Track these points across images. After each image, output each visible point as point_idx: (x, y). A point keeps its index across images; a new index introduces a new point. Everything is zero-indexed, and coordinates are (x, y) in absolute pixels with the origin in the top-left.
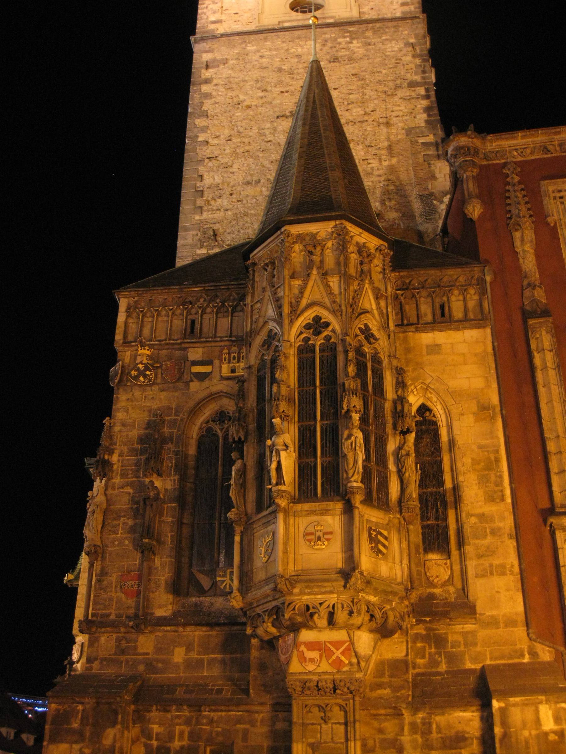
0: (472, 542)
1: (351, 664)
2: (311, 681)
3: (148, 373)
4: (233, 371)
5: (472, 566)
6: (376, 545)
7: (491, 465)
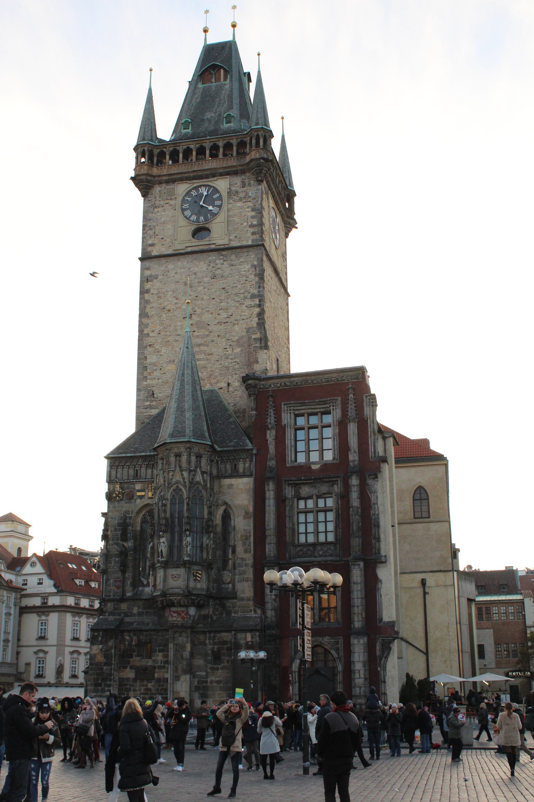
5: (237, 577)
7: (247, 538)
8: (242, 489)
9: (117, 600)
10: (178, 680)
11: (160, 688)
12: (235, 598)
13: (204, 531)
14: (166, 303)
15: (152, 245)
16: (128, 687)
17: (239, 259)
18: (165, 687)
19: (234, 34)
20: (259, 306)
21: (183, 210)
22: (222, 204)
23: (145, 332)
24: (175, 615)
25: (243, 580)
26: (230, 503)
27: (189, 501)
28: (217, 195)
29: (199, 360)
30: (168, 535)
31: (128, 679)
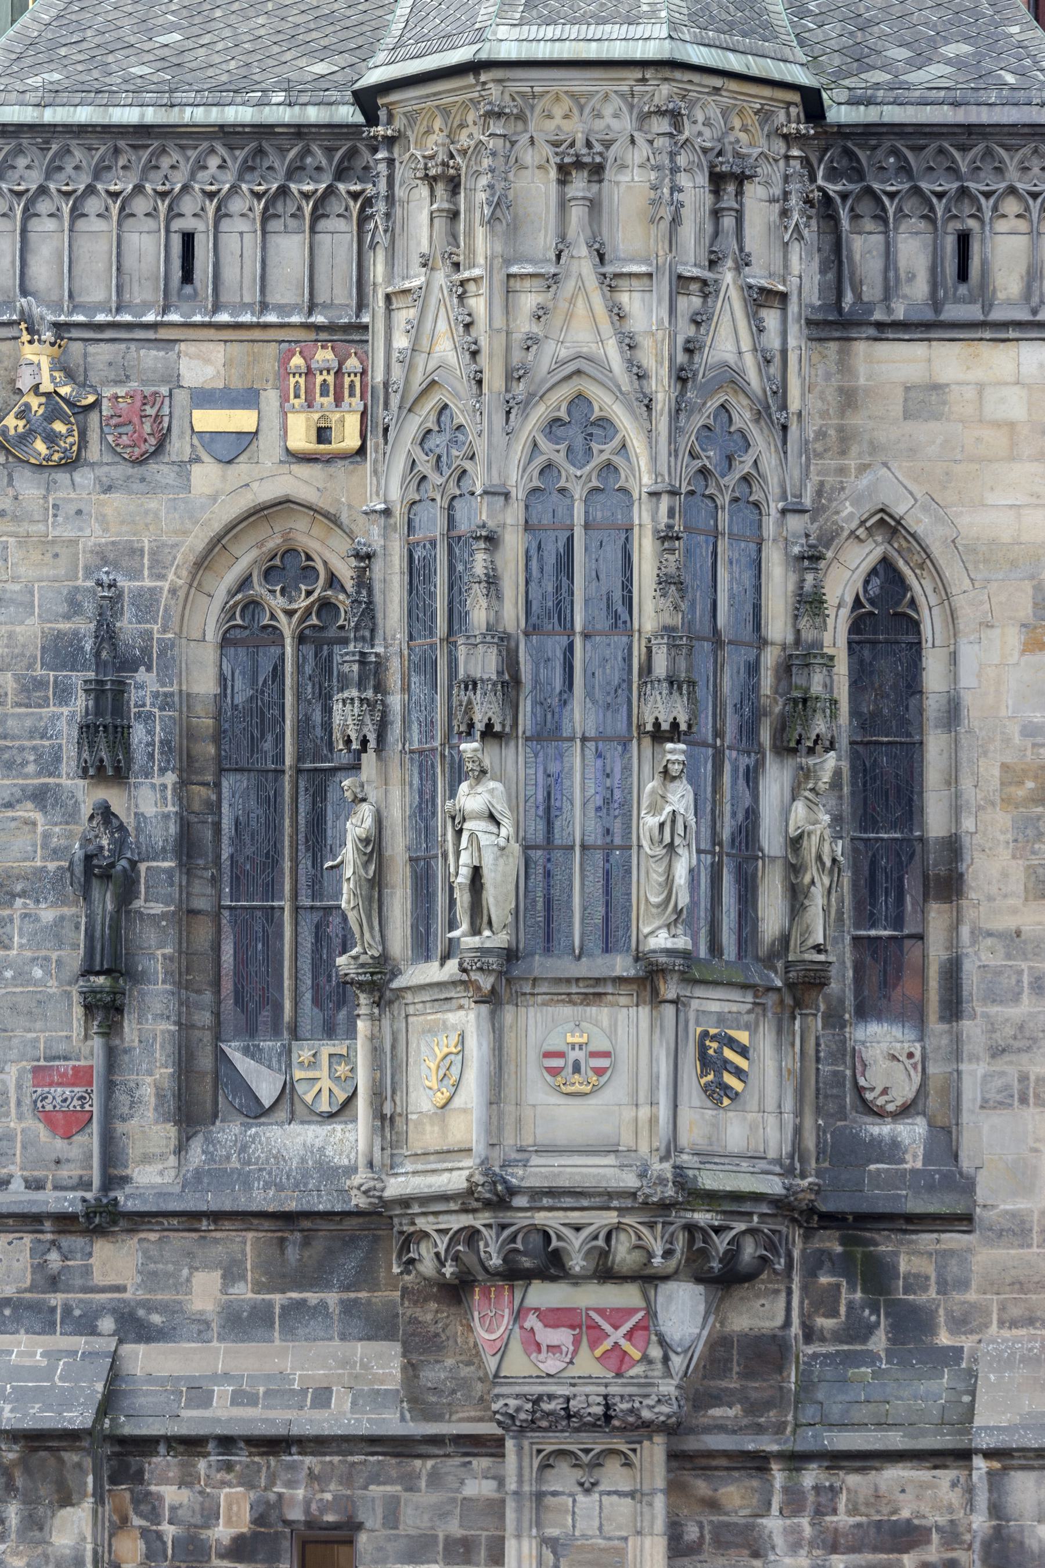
3: (59, 427)
4: (323, 434)
5: (975, 1074)
9: (65, 1222)
12: (963, 1221)
13: (766, 736)
24: (562, 1337)
26: (920, 523)
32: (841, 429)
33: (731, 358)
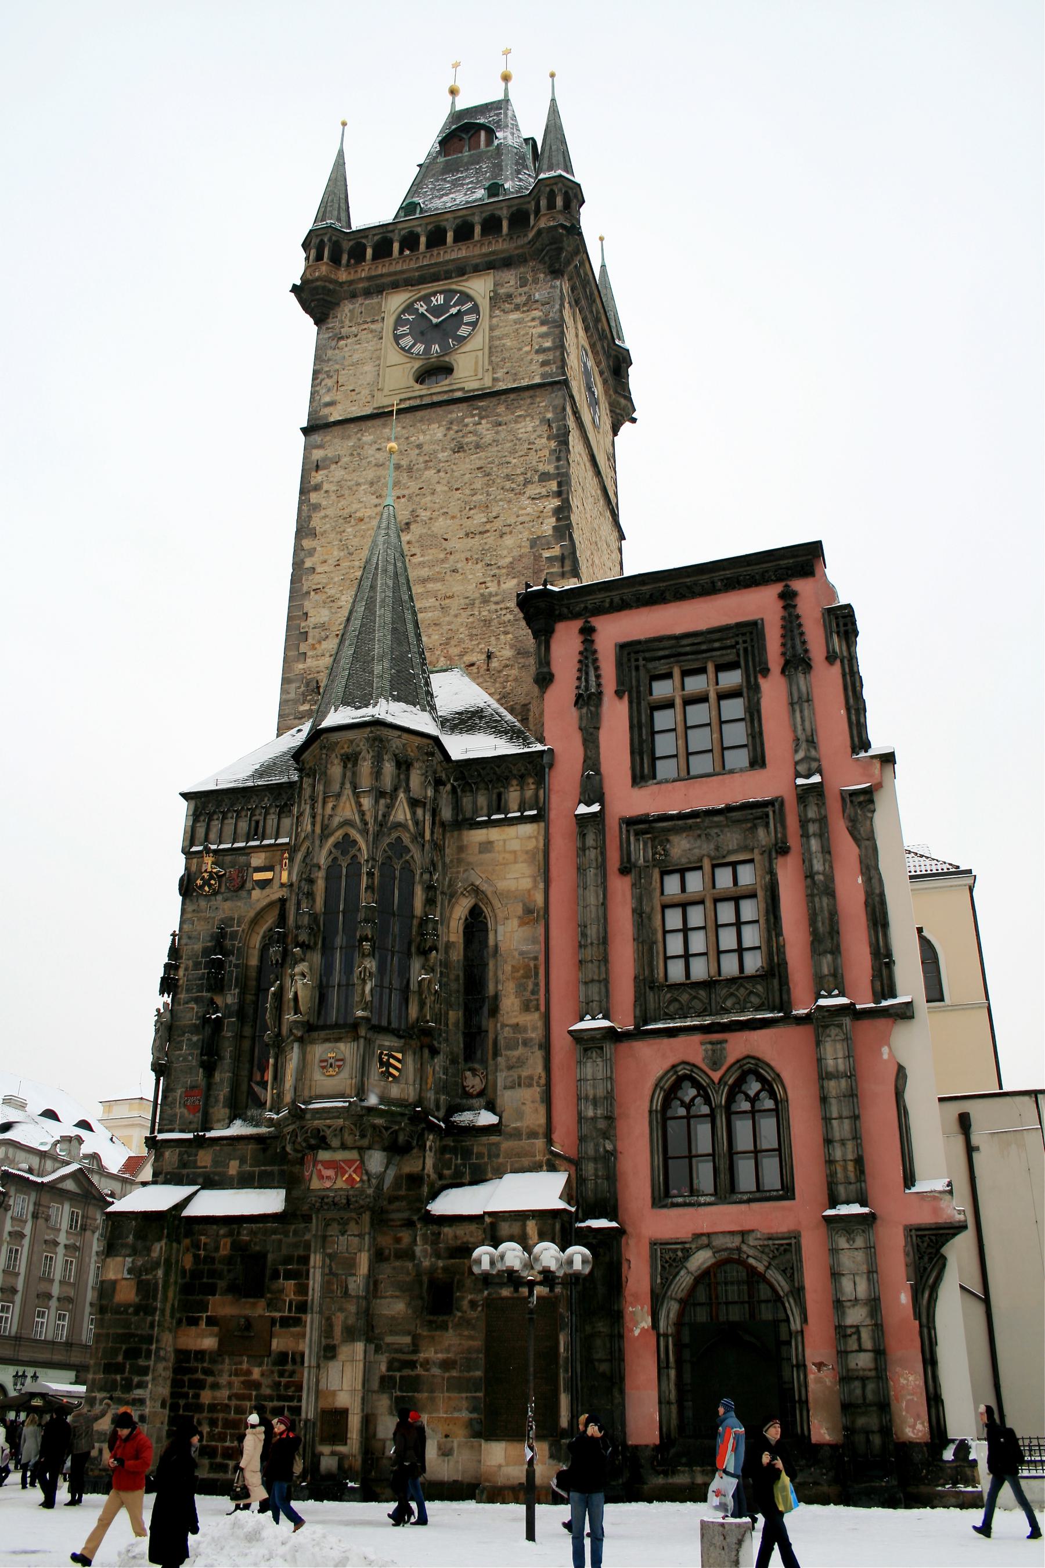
0: (504, 1053)
1: (362, 1180)
2: (328, 1197)
5: (501, 1078)
6: (387, 1069)
8: (515, 852)
10: (333, 1357)
11: (283, 1380)
13: (413, 950)
14: (355, 506)
15: (331, 404)
16: (200, 1376)
17: (513, 413)
18: (295, 1379)
19: (506, 89)
20: (559, 494)
21: (397, 338)
22: (478, 319)
23: (308, 564)
24: (330, 1173)
25: (518, 1083)
27: (373, 867)
28: (469, 305)
29: (424, 610)
30: (316, 957)
31: (200, 1354)
32: (458, 859)
33: (403, 822)
